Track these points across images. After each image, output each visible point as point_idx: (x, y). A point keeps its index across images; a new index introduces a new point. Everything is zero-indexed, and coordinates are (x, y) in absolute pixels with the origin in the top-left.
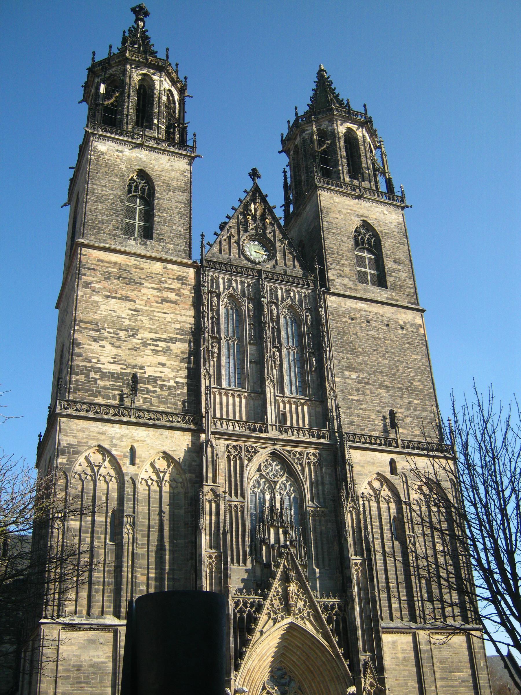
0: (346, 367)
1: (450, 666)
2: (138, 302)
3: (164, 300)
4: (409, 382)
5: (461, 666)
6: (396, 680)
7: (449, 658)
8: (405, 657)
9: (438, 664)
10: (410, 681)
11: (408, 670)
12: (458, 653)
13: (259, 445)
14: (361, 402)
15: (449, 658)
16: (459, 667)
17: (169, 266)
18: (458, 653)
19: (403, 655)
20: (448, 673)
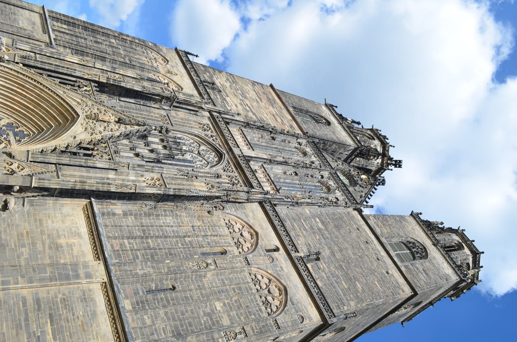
0: (322, 221)
1: (60, 315)
2: (263, 104)
3: (273, 115)
4: (353, 276)
5: (64, 336)
6: (27, 232)
7: (73, 315)
8: (61, 247)
9: (60, 296)
10: (28, 251)
11: (44, 251)
12: (84, 331)
13: (221, 144)
14: (305, 229)
15: (73, 315)
16: (62, 332)
17: (294, 122)
18: (84, 331)
19: (64, 244)
20: (48, 312)
